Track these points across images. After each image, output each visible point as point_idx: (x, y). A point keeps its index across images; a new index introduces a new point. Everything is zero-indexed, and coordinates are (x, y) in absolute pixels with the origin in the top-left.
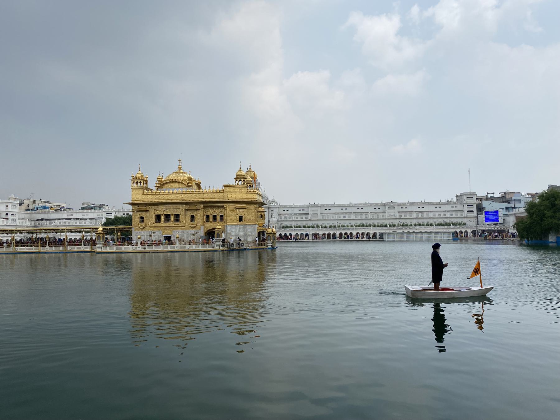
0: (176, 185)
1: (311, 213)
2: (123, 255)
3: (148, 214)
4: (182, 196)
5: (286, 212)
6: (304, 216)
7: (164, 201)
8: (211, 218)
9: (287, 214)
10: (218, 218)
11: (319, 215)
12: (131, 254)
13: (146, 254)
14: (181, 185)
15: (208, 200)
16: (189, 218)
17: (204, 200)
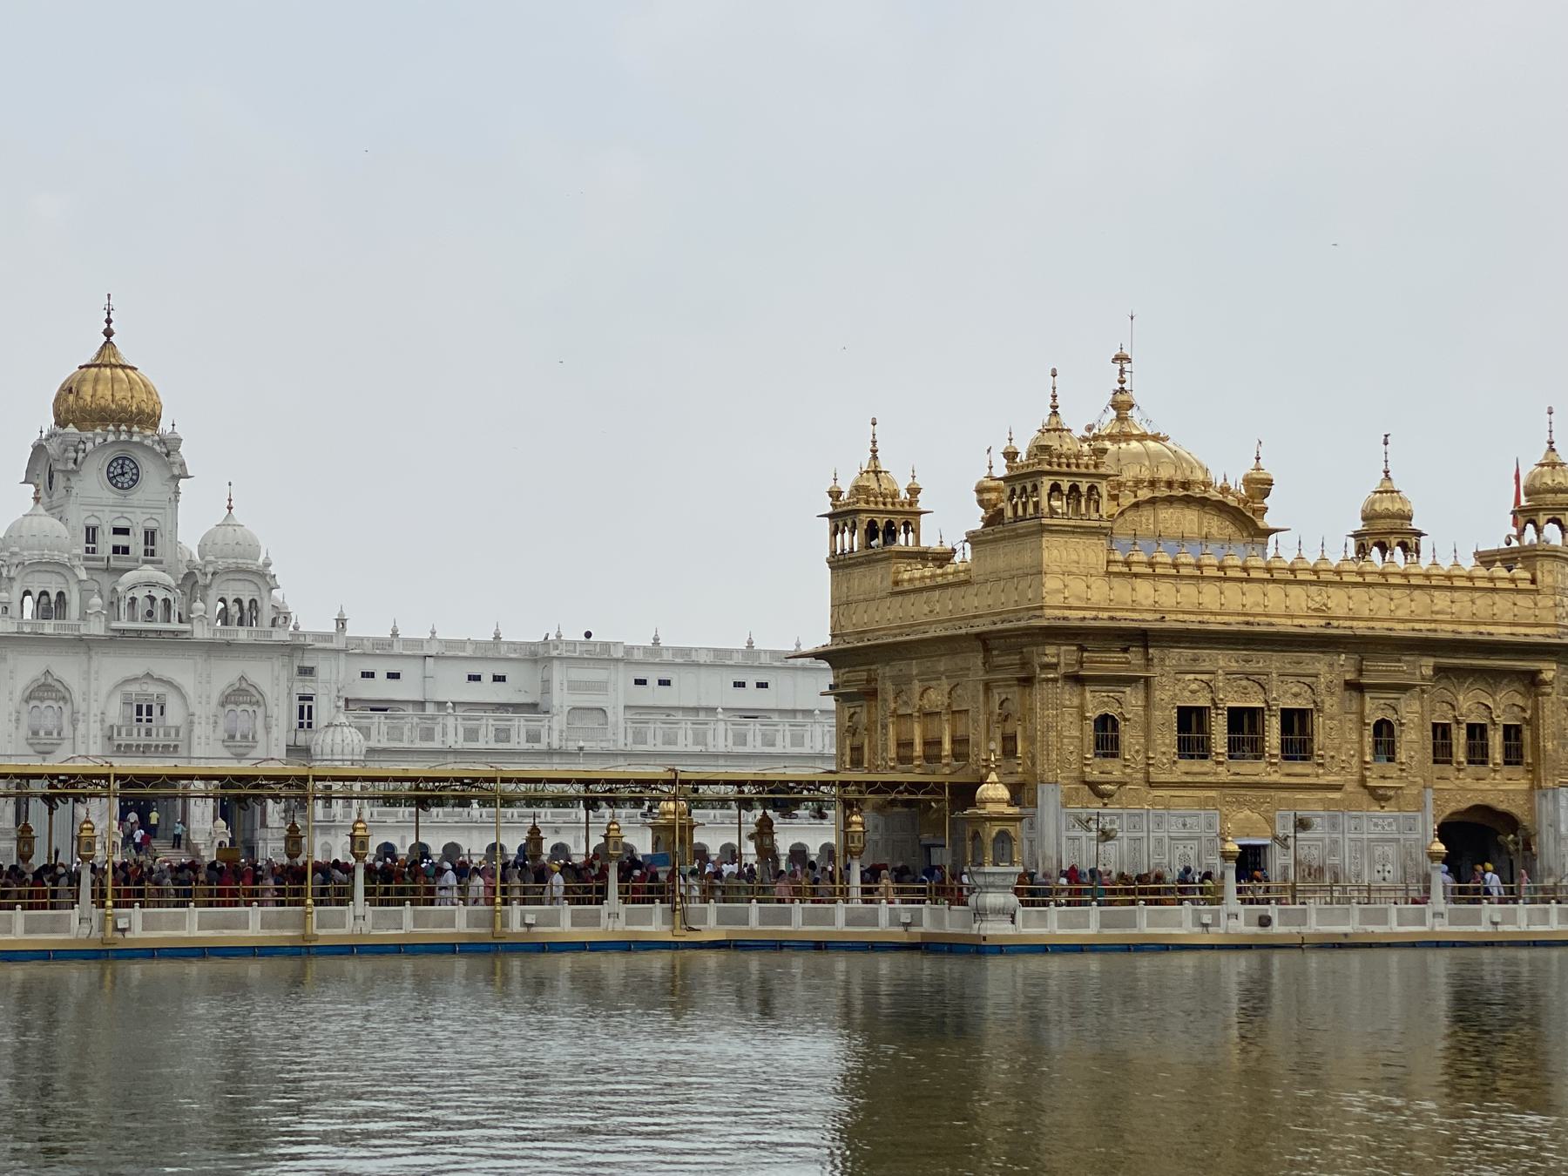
0: (1189, 520)
1: (561, 699)
2: (1144, 963)
3: (1133, 698)
4: (1317, 596)
5: (380, 689)
6: (519, 725)
7: (1235, 624)
8: (1460, 738)
9: (379, 707)
10: (1496, 740)
11: (617, 716)
12: (1188, 960)
13: (1277, 959)
14: (1215, 525)
15: (1467, 632)
16: (1369, 739)
17: (1445, 631)
